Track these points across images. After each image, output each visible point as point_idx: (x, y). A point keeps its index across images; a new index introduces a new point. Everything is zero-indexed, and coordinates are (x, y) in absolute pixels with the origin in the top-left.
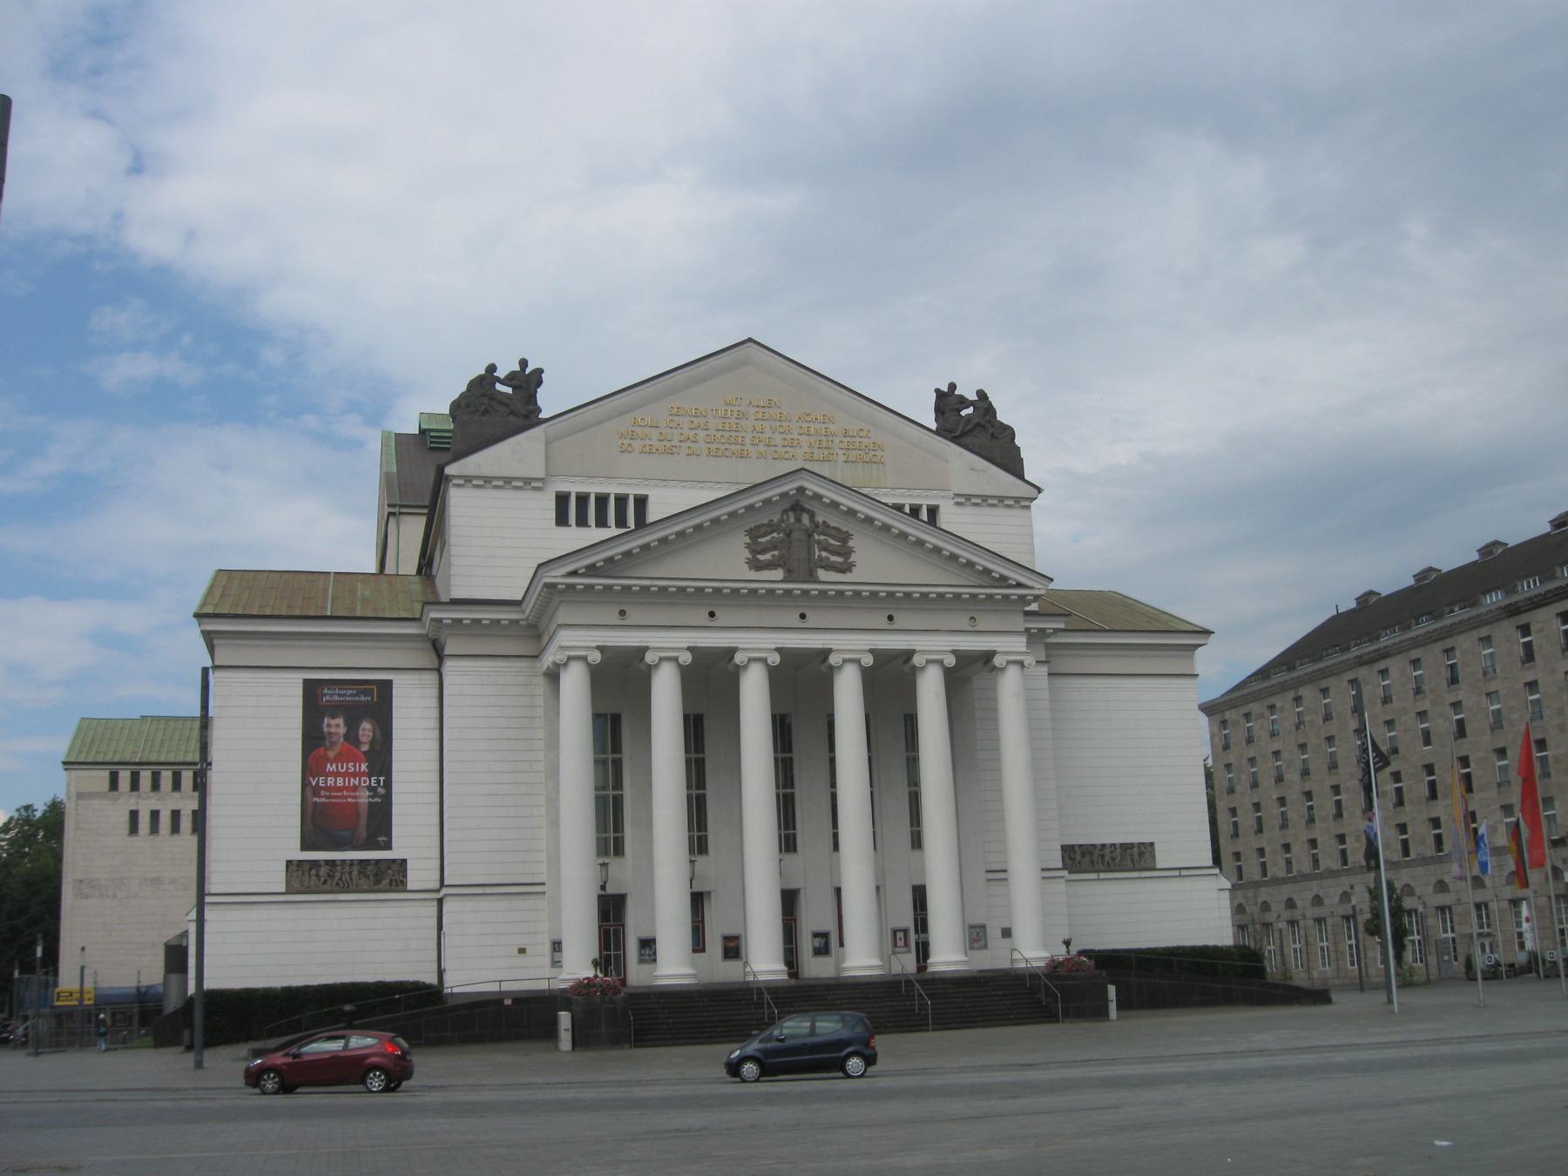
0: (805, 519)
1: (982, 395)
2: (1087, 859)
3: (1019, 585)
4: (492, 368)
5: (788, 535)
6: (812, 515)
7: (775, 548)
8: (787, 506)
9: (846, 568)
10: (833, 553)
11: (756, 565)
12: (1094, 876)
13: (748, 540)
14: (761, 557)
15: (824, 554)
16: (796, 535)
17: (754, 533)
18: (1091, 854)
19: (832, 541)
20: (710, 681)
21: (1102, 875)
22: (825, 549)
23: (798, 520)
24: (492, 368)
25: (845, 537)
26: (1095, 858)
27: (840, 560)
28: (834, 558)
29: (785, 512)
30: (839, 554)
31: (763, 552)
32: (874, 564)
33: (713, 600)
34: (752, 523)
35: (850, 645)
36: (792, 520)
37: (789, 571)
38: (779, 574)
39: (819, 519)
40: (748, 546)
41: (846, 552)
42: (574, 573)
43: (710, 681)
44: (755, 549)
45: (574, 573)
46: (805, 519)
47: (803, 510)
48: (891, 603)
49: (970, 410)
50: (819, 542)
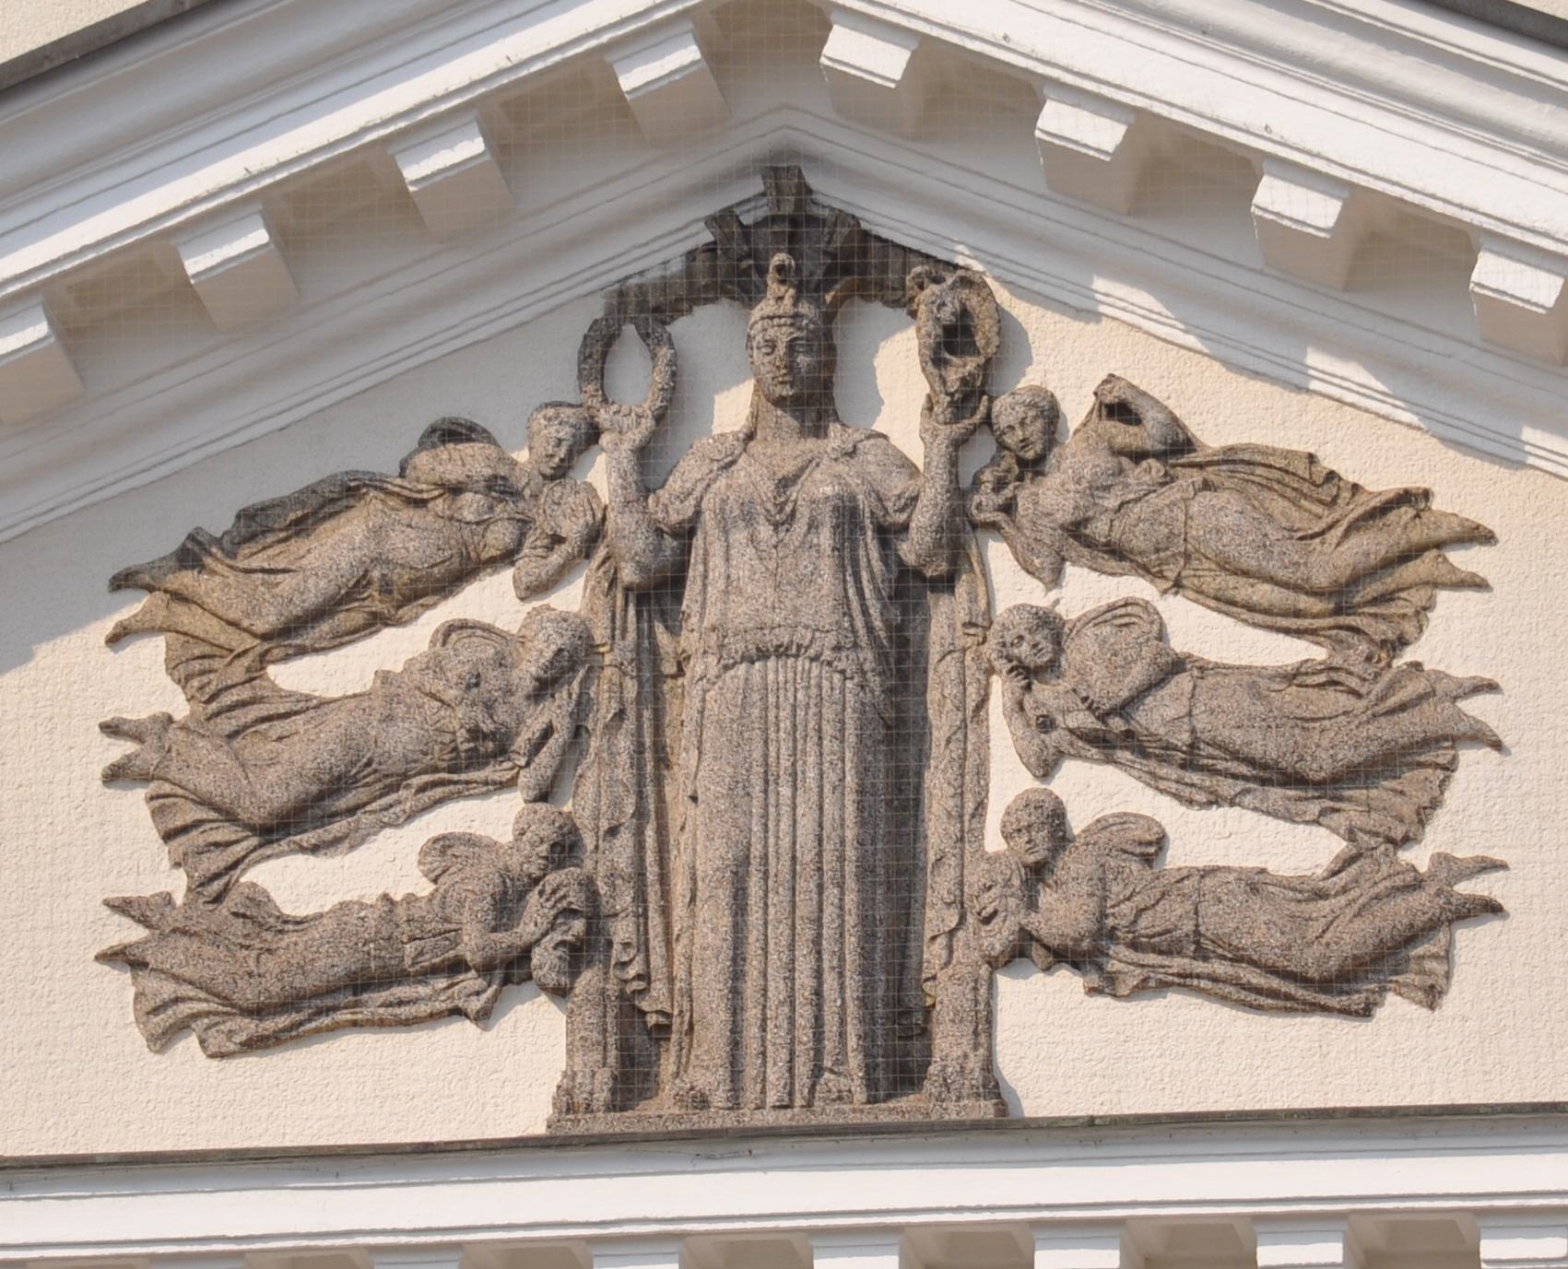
0: (896, 377)
5: (660, 592)
7: (475, 757)
8: (664, 244)
10: (1197, 766)
13: (146, 683)
14: (295, 882)
15: (1095, 792)
16: (734, 586)
19: (1195, 628)
22: (1113, 737)
23: (811, 395)
27: (1299, 847)
29: (646, 310)
30: (1283, 781)
31: (307, 818)
37: (634, 1047)
39: (1064, 362)
40: (140, 760)
46: (896, 377)
47: (855, 269)
50: (1039, 654)
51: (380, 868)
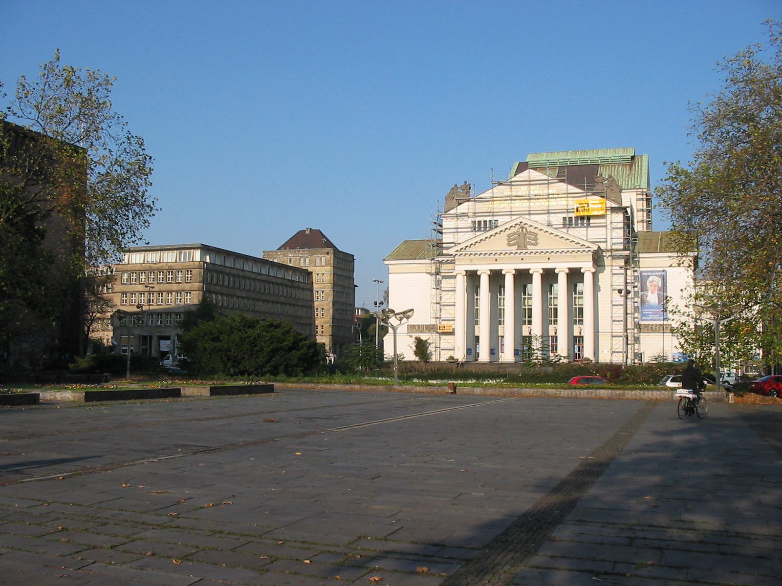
1: (610, 176)
2: (646, 329)
3: (588, 247)
4: (456, 186)
6: (526, 229)
9: (536, 244)
10: (532, 240)
11: (509, 245)
12: (647, 334)
15: (530, 241)
17: (509, 236)
18: (648, 327)
20: (497, 278)
21: (650, 334)
23: (522, 230)
24: (456, 186)
25: (536, 235)
26: (649, 328)
28: (532, 242)
32: (545, 243)
33: (495, 255)
34: (508, 232)
35: (536, 269)
36: (521, 231)
37: (519, 246)
38: (516, 246)
39: (528, 230)
40: (507, 240)
41: (536, 239)
42: (457, 251)
43: (497, 278)
44: (509, 240)
45: (457, 251)
47: (524, 227)
48: (549, 254)
49: (606, 182)
51: (513, 242)
